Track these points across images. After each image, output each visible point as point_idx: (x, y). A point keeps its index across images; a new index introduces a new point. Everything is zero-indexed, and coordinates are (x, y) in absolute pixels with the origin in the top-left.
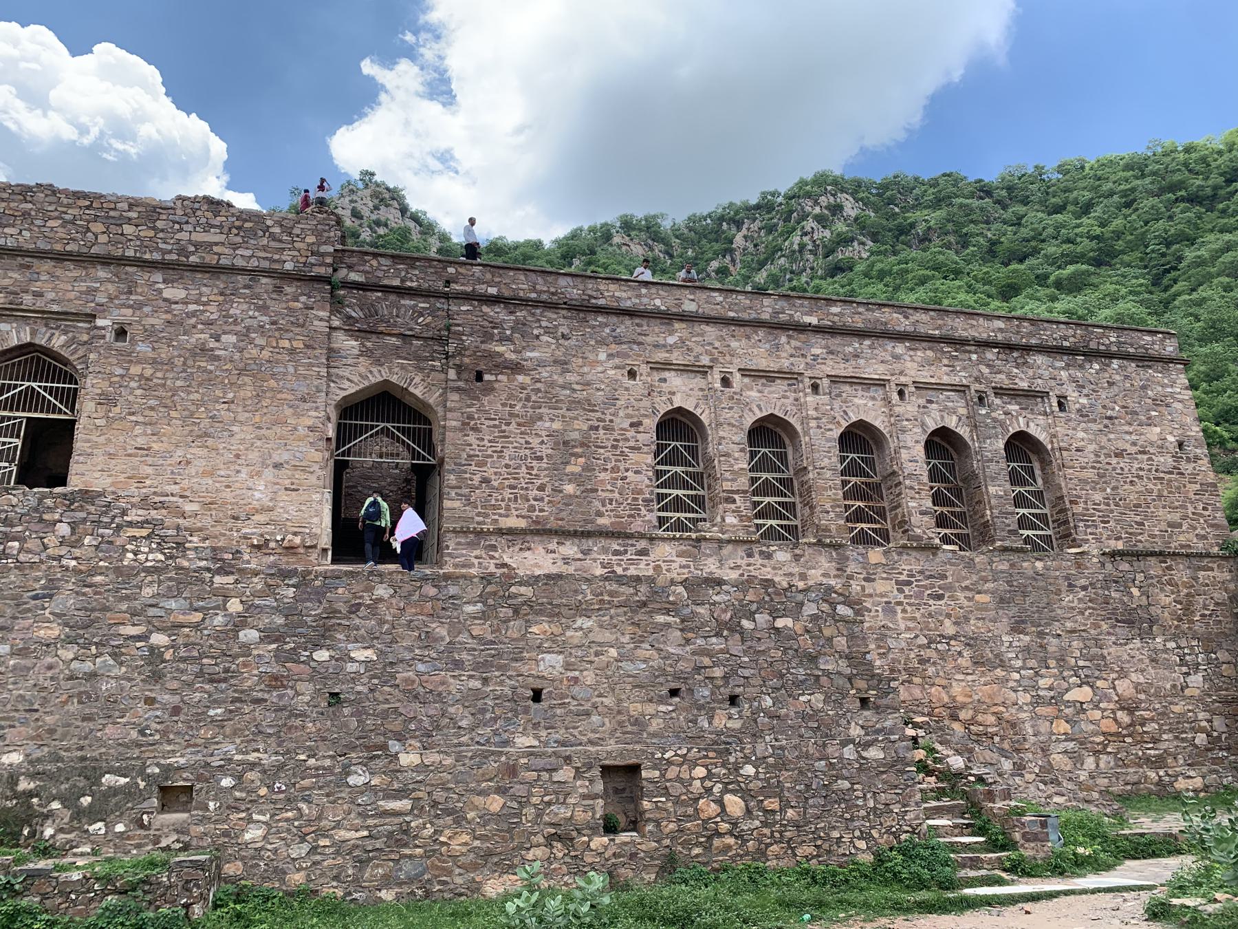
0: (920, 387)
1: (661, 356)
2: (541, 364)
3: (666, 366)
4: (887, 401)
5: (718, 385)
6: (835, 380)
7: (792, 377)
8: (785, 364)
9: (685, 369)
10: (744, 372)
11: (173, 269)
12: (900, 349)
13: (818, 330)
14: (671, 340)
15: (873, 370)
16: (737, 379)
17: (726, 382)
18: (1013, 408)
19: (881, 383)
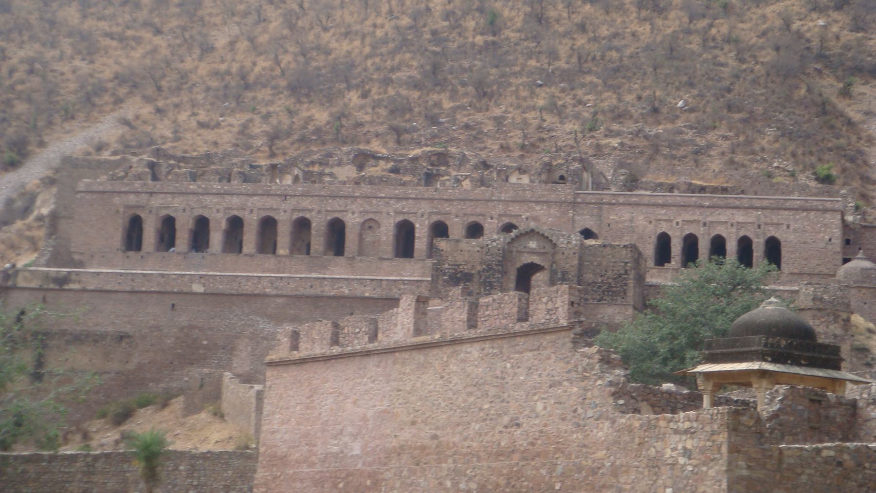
0: (738, 223)
1: (659, 217)
2: (625, 221)
3: (660, 220)
4: (727, 228)
5: (674, 225)
6: (711, 222)
7: (697, 222)
8: (696, 218)
9: (666, 220)
10: (683, 221)
11: (538, 202)
12: (734, 211)
13: (708, 207)
14: (663, 212)
15: (722, 218)
16: (680, 223)
17: (677, 223)
18: (771, 228)
19: (726, 222)
